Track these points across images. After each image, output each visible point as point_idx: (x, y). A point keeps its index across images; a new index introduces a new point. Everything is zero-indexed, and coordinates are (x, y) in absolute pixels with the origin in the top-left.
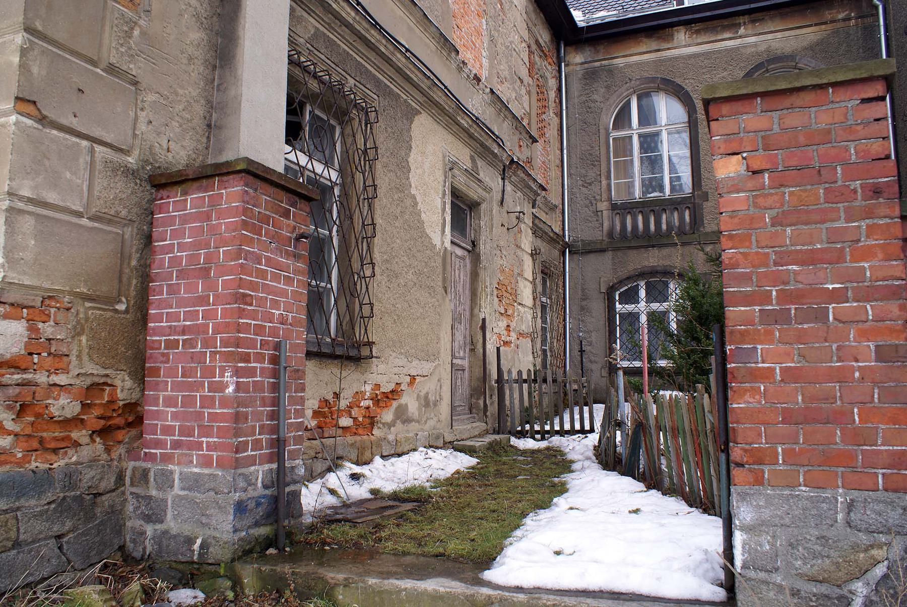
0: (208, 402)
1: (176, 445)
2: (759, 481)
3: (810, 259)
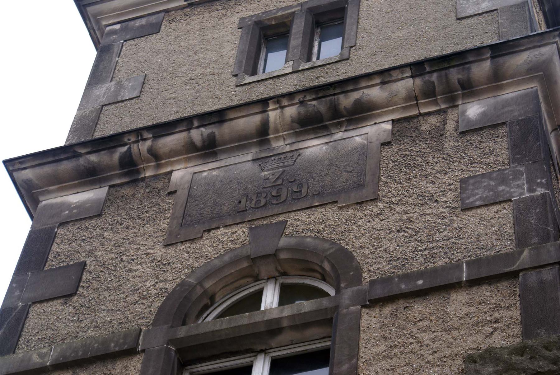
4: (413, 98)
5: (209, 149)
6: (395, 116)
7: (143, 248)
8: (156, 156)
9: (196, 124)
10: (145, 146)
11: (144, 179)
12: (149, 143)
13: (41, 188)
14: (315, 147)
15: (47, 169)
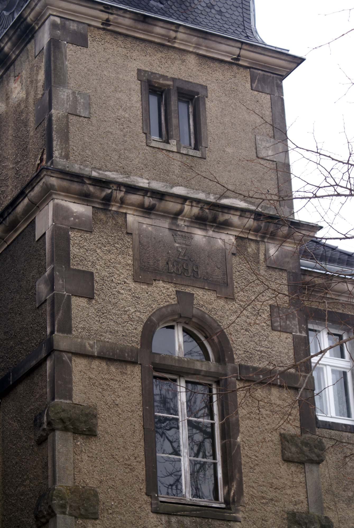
5: (148, 211)
6: (237, 234)
7: (123, 276)
8: (122, 202)
9: (149, 194)
10: (120, 195)
11: (110, 210)
12: (122, 194)
13: (56, 191)
14: (199, 236)
15: (65, 184)
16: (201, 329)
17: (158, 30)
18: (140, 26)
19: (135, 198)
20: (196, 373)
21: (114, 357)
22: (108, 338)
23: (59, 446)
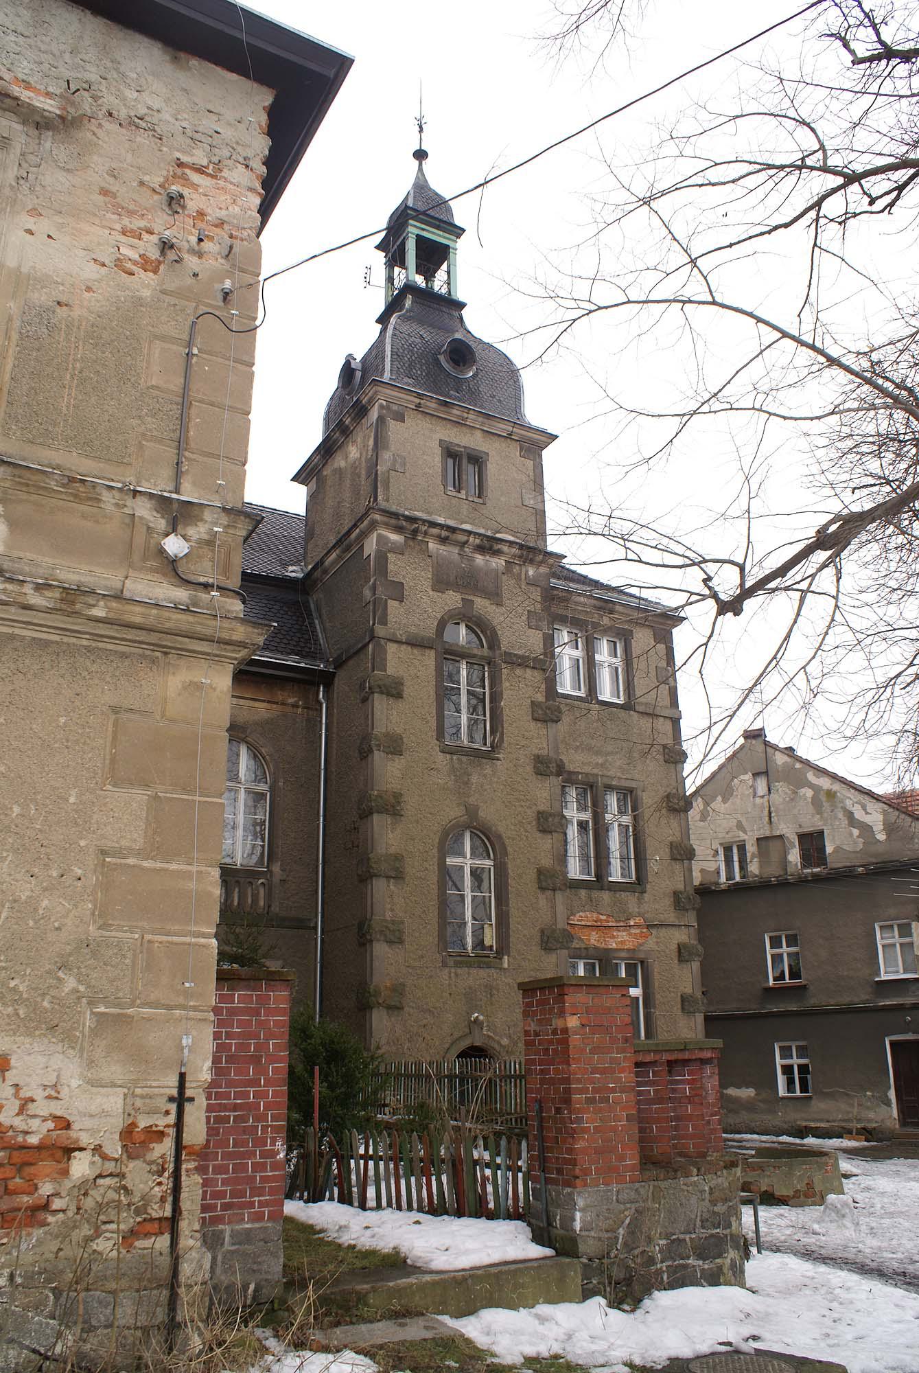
0: (258, 1167)
1: (226, 1207)
2: (586, 1185)
3: (603, 1071)
4: (515, 556)
5: (443, 540)
8: (426, 533)
14: (479, 559)
15: (385, 519)
16: (478, 626)
17: (455, 412)
18: (442, 408)
19: (435, 531)
20: (474, 656)
21: (416, 643)
22: (413, 629)
23: (376, 704)
